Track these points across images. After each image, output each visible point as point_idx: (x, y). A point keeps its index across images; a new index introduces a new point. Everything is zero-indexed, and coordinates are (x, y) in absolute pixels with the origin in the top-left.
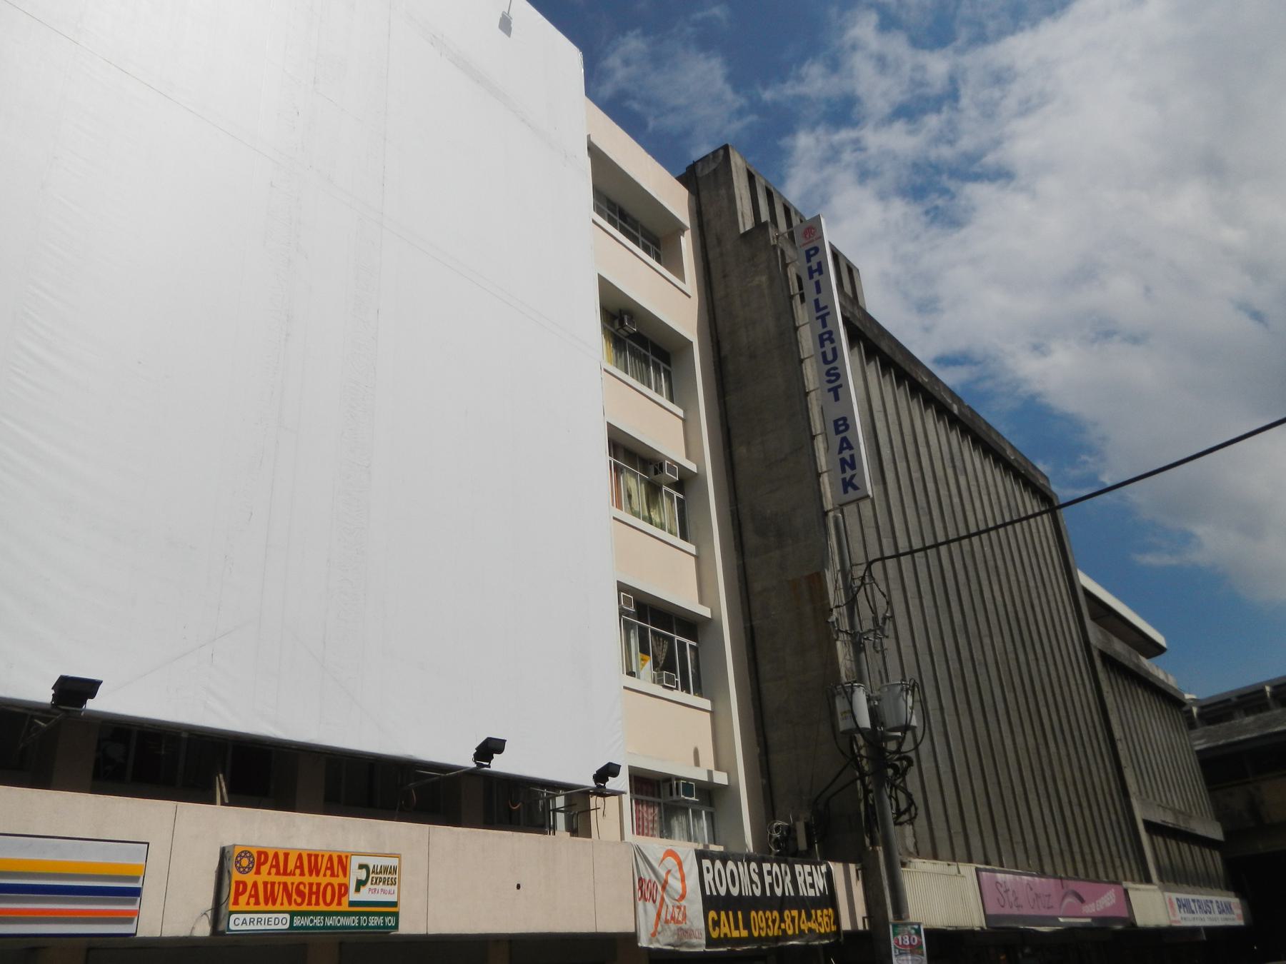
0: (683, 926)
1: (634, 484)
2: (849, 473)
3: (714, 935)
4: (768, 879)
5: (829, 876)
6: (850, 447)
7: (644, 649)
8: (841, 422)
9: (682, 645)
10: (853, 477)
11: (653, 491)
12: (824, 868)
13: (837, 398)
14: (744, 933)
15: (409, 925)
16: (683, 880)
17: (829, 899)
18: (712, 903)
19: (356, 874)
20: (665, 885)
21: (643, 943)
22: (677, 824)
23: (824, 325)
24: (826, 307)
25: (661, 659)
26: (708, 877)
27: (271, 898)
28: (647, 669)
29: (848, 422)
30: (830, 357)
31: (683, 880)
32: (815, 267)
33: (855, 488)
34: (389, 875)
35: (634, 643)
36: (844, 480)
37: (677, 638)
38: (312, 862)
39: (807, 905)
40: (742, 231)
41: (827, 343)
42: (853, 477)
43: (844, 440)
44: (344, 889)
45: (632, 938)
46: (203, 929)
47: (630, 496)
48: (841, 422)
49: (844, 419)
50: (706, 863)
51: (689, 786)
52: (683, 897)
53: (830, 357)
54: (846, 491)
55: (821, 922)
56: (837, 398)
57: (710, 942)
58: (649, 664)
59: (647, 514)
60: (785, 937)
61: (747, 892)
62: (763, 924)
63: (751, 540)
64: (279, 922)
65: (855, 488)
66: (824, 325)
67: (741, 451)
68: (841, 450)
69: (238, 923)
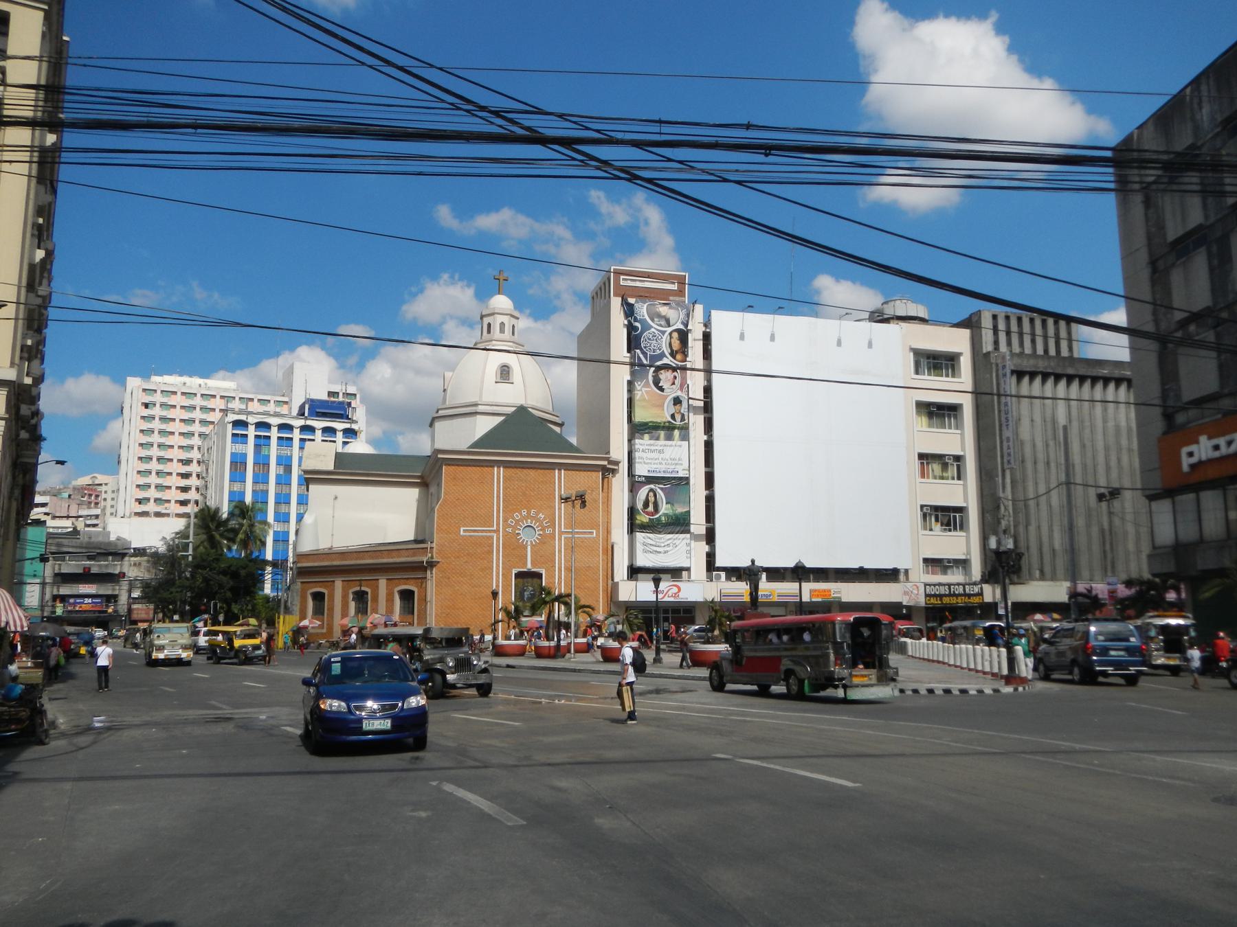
0: (918, 601)
1: (936, 467)
3: (928, 602)
4: (952, 590)
5: (982, 589)
7: (937, 520)
9: (955, 517)
11: (945, 466)
12: (979, 586)
14: (940, 602)
15: (843, 600)
16: (918, 591)
17: (981, 594)
18: (927, 595)
19: (832, 592)
20: (912, 592)
21: (904, 604)
22: (949, 571)
25: (945, 521)
26: (928, 591)
27: (818, 596)
28: (937, 527)
31: (918, 591)
34: (839, 592)
35: (933, 519)
37: (952, 515)
38: (825, 591)
39: (969, 596)
40: (984, 351)
44: (830, 595)
45: (901, 603)
46: (809, 601)
47: (933, 471)
50: (927, 587)
51: (949, 561)
52: (917, 594)
55: (976, 600)
57: (926, 604)
58: (939, 524)
59: (941, 474)
60: (958, 603)
61: (941, 593)
62: (946, 600)
63: (984, 477)
64: (820, 600)
67: (982, 444)
69: (813, 600)
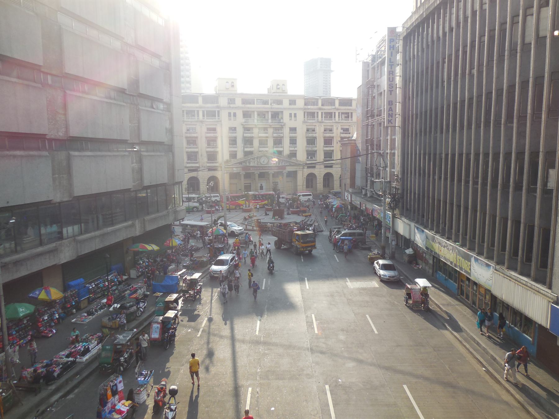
2: (390, 118)
6: (392, 110)
8: (391, 102)
10: (391, 120)
13: (391, 94)
23: (391, 68)
24: (393, 62)
29: (393, 103)
30: (391, 80)
32: (392, 46)
33: (392, 123)
36: (388, 120)
41: (391, 75)
42: (391, 120)
43: (391, 108)
48: (391, 102)
49: (392, 101)
53: (391, 80)
54: (389, 123)
56: (391, 94)
65: (392, 123)
66: (391, 68)
68: (389, 111)
